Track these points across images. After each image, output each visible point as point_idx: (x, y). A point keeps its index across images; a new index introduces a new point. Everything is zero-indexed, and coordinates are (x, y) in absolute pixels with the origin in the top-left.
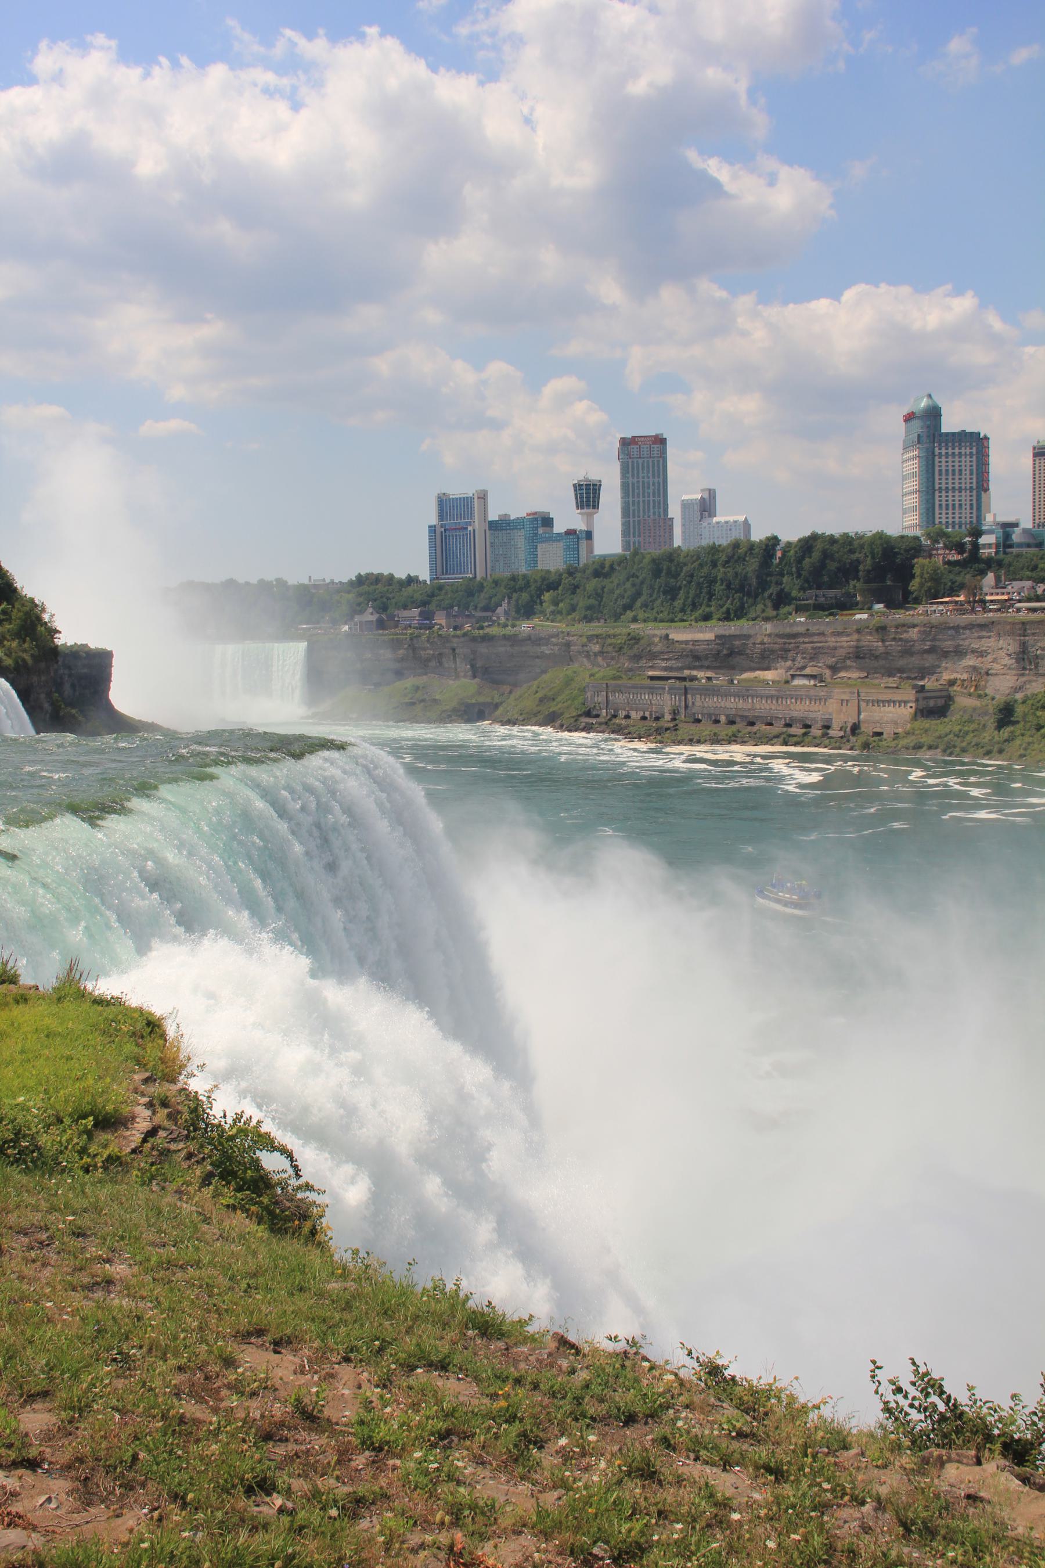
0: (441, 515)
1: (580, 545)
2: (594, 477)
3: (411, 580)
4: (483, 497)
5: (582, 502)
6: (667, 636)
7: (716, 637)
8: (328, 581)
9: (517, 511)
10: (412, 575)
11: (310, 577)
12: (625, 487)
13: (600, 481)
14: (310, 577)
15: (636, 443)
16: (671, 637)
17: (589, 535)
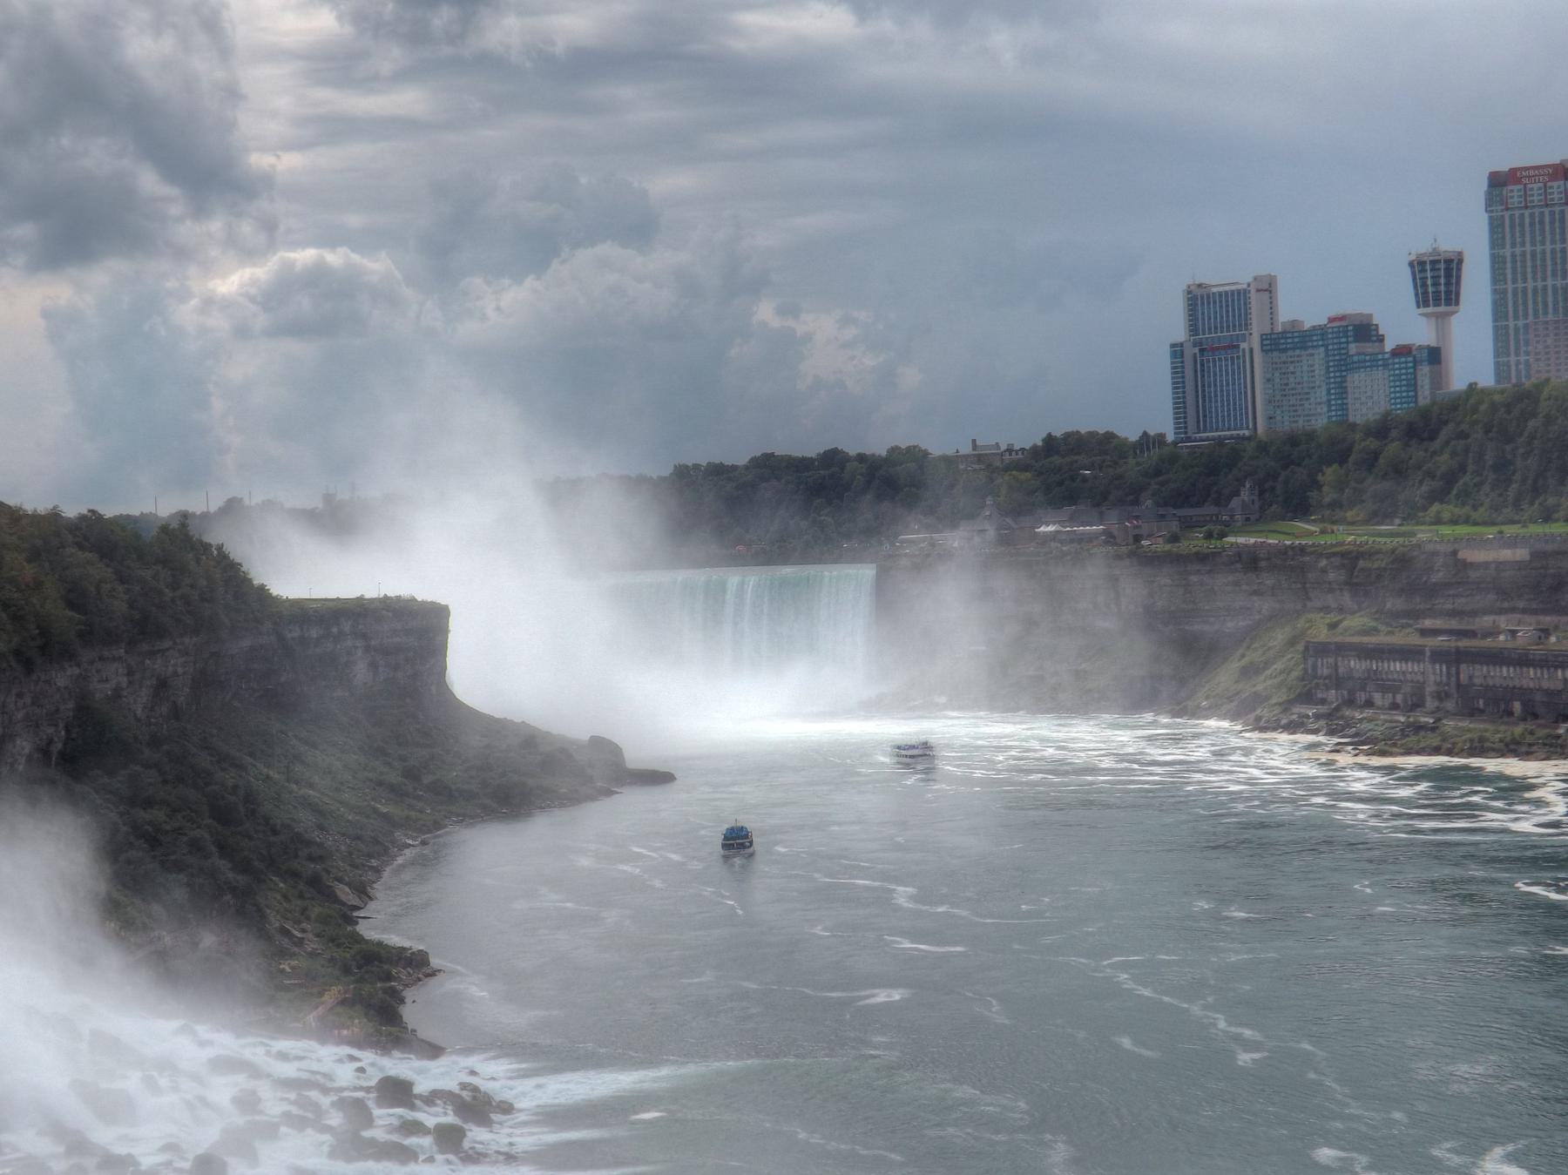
0: (1193, 328)
1: (1419, 374)
2: (1448, 246)
3: (1148, 442)
4: (1268, 287)
5: (1425, 293)
6: (1455, 553)
7: (1532, 554)
8: (1003, 447)
9: (1312, 317)
10: (1152, 433)
11: (974, 441)
12: (1497, 263)
13: (1460, 254)
14: (974, 441)
15: (1518, 181)
16: (1461, 555)
17: (1435, 356)
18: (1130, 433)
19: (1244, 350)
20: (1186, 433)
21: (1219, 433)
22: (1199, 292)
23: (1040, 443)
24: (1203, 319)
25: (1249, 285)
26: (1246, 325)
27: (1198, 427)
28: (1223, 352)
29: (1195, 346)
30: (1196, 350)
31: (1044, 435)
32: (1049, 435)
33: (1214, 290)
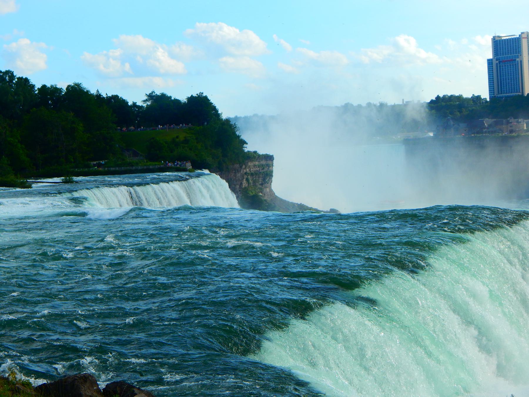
3: (477, 99)
11: (403, 100)
18: (467, 94)
19: (518, 61)
20: (494, 94)
21: (508, 94)
22: (497, 39)
23: (434, 99)
24: (500, 50)
25: (520, 35)
26: (519, 51)
27: (499, 92)
28: (509, 62)
29: (497, 60)
30: (498, 62)
31: (436, 96)
32: (438, 96)
33: (503, 38)
